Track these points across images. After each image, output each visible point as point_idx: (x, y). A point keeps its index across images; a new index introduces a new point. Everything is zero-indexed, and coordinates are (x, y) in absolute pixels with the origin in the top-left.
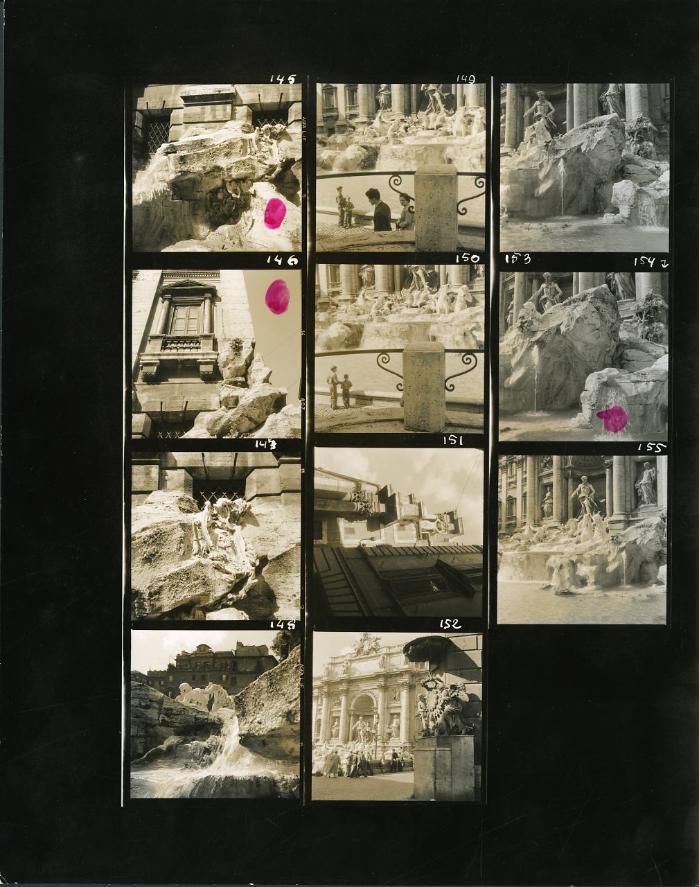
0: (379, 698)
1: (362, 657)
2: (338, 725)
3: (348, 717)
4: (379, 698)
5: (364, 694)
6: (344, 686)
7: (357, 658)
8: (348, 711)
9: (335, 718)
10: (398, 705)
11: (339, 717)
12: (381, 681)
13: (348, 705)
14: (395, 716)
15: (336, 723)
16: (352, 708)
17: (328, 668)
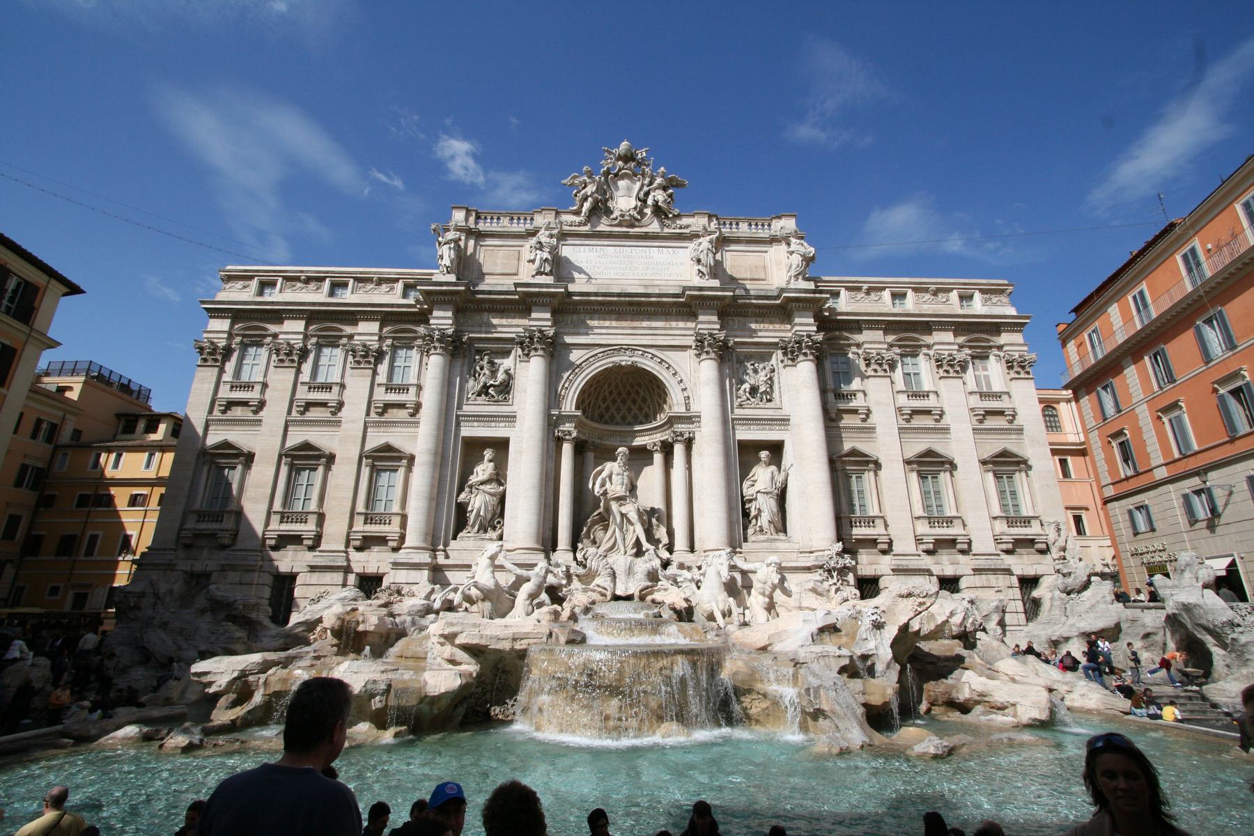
0: (693, 382)
1: (602, 227)
2: (499, 477)
3: (552, 444)
4: (693, 382)
5: (624, 359)
6: (541, 319)
7: (587, 228)
8: (551, 422)
9: (474, 448)
10: (770, 413)
11: (501, 446)
12: (708, 323)
13: (552, 397)
14: (764, 454)
15: (483, 470)
16: (569, 406)
17: (457, 241)
